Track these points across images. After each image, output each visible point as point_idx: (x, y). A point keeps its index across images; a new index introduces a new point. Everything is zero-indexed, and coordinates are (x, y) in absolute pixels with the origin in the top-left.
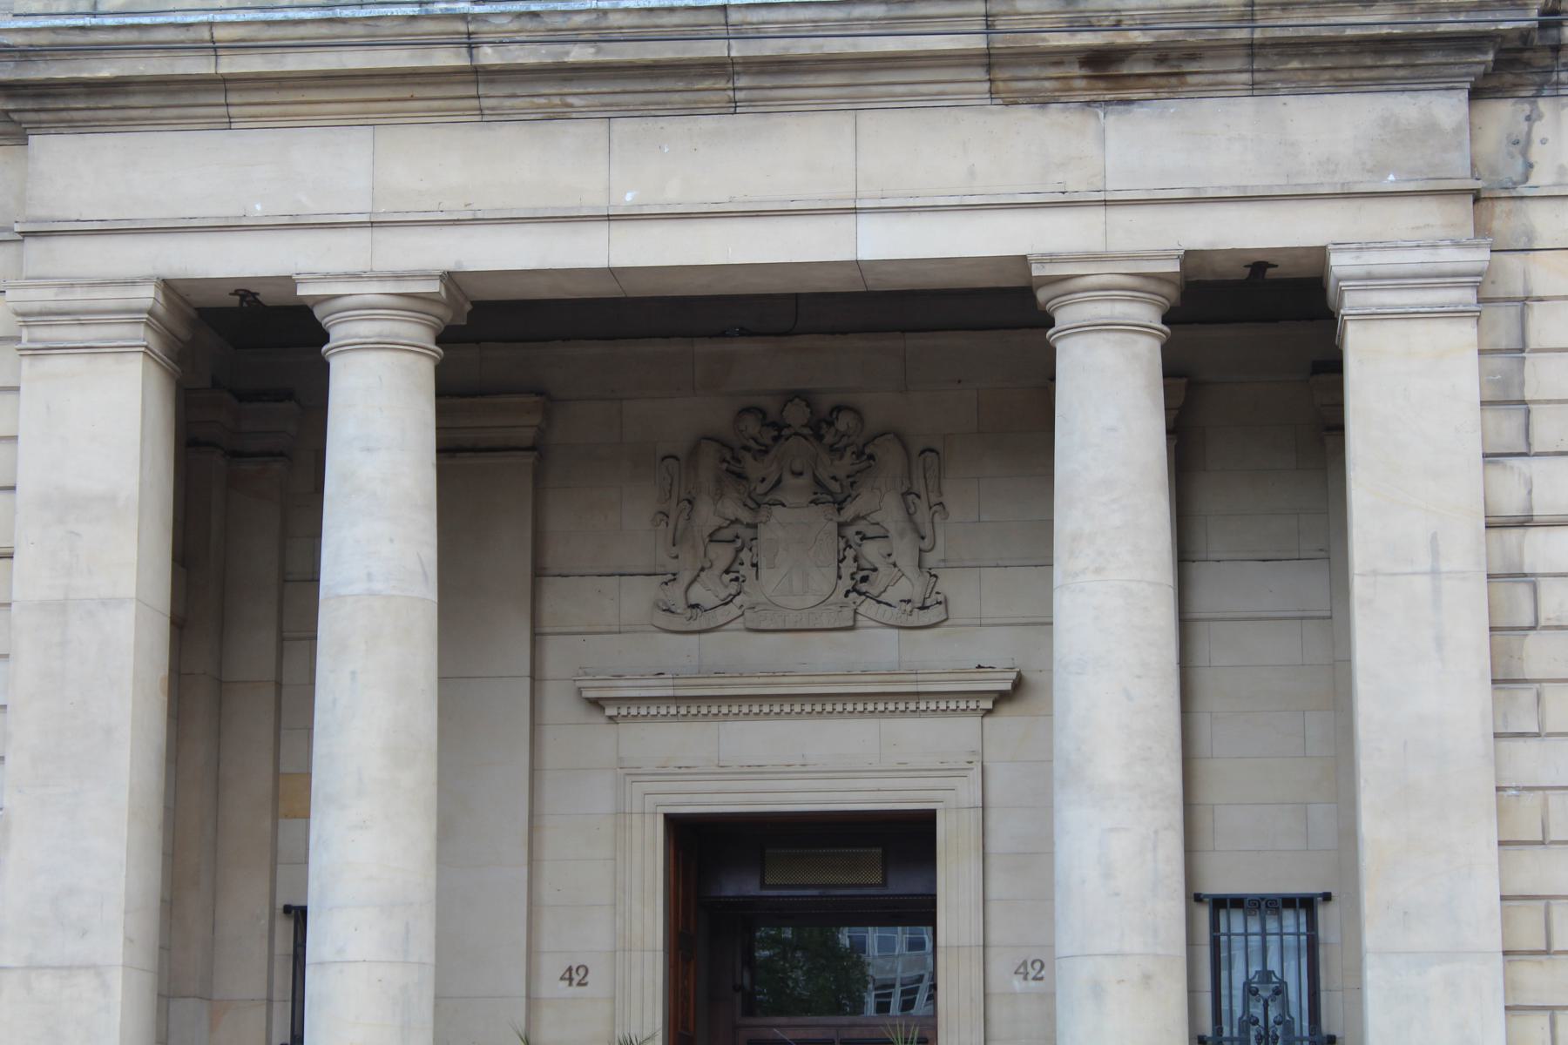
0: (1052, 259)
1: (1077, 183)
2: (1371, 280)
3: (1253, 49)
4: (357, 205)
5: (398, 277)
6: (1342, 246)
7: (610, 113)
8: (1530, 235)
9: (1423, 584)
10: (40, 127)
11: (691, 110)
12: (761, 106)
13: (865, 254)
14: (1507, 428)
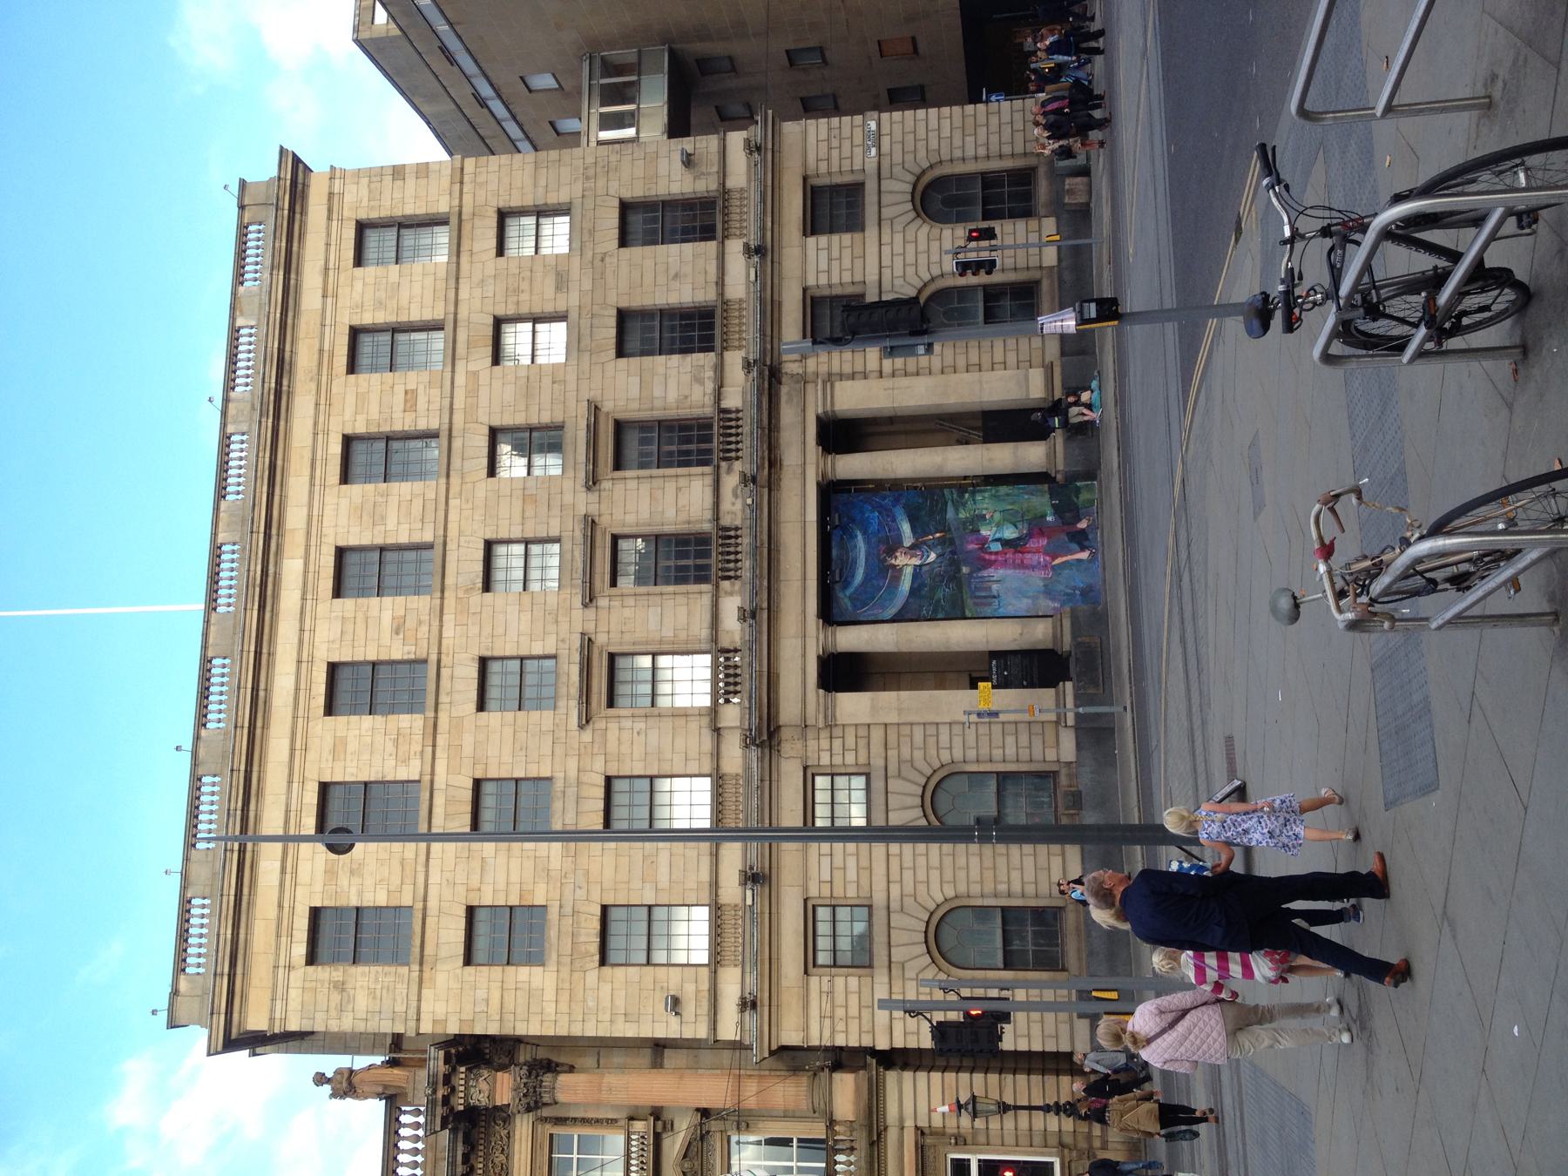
0: (817, 475)
1: (799, 471)
2: (824, 405)
3: (770, 430)
4: (799, 642)
5: (818, 629)
6: (816, 410)
7: (778, 580)
8: (814, 373)
9: (895, 391)
10: (777, 721)
11: (778, 561)
12: (778, 546)
13: (815, 518)
14: (857, 376)
